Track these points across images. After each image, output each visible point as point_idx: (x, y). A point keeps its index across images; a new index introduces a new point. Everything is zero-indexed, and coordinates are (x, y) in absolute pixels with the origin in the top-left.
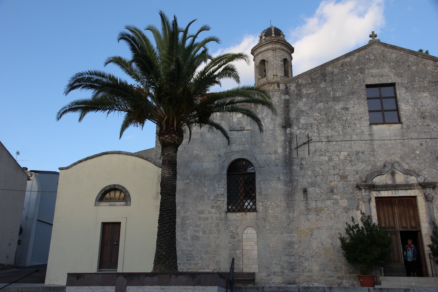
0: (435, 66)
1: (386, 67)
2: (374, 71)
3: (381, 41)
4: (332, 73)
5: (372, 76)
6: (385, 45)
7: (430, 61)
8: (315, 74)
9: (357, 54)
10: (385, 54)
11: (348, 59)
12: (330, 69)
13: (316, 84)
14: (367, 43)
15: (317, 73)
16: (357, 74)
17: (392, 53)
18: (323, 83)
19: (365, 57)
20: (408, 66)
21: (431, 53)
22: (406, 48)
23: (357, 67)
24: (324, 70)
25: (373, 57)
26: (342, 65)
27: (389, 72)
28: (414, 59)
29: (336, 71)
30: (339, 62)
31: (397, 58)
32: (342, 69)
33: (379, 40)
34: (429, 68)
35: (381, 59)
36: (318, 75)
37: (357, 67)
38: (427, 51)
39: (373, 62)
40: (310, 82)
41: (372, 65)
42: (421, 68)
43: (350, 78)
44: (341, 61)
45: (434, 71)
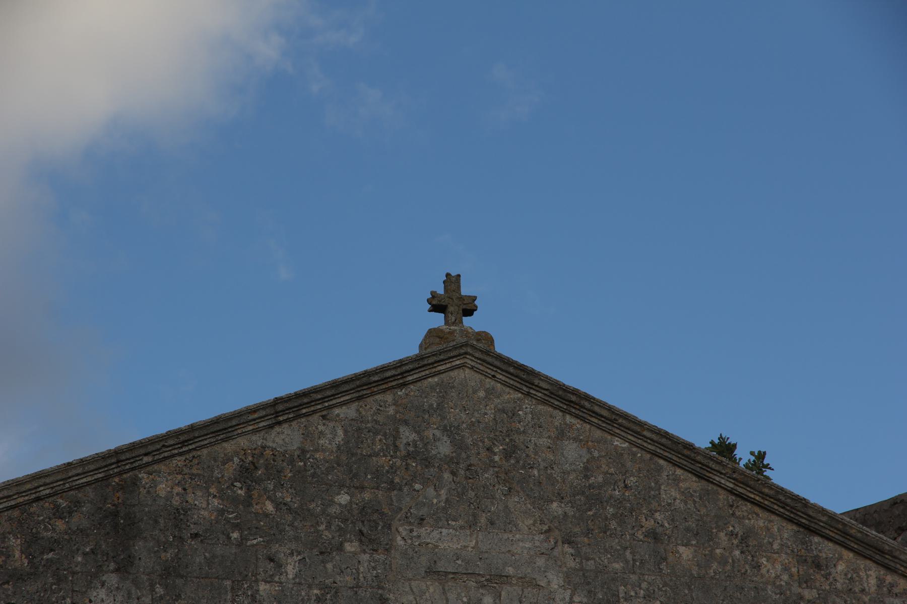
0: (802, 561)
1: (525, 523)
2: (449, 541)
3: (501, 348)
4: (179, 516)
5: (431, 572)
6: (524, 378)
7: (776, 524)
8: (58, 513)
9: (350, 412)
10: (519, 439)
11: (286, 438)
12: (162, 489)
13: (59, 580)
14: (413, 350)
15: (78, 503)
16: (340, 548)
17: (561, 434)
18: (112, 579)
19: (396, 436)
20: (654, 536)
21: (782, 475)
22: (642, 417)
23: (343, 499)
24: (122, 487)
25: (444, 448)
26: (246, 473)
27: (541, 562)
28: (687, 495)
29: (205, 506)
30: (229, 447)
31: (587, 472)
32: (248, 501)
33: (487, 338)
34: (771, 568)
35: (492, 464)
36: (78, 520)
37: (343, 499)
38: (761, 456)
39: (447, 476)
40: (19, 560)
41: (436, 497)
42: (723, 561)
43: (291, 570)
44: (243, 442)
45: (796, 589)
